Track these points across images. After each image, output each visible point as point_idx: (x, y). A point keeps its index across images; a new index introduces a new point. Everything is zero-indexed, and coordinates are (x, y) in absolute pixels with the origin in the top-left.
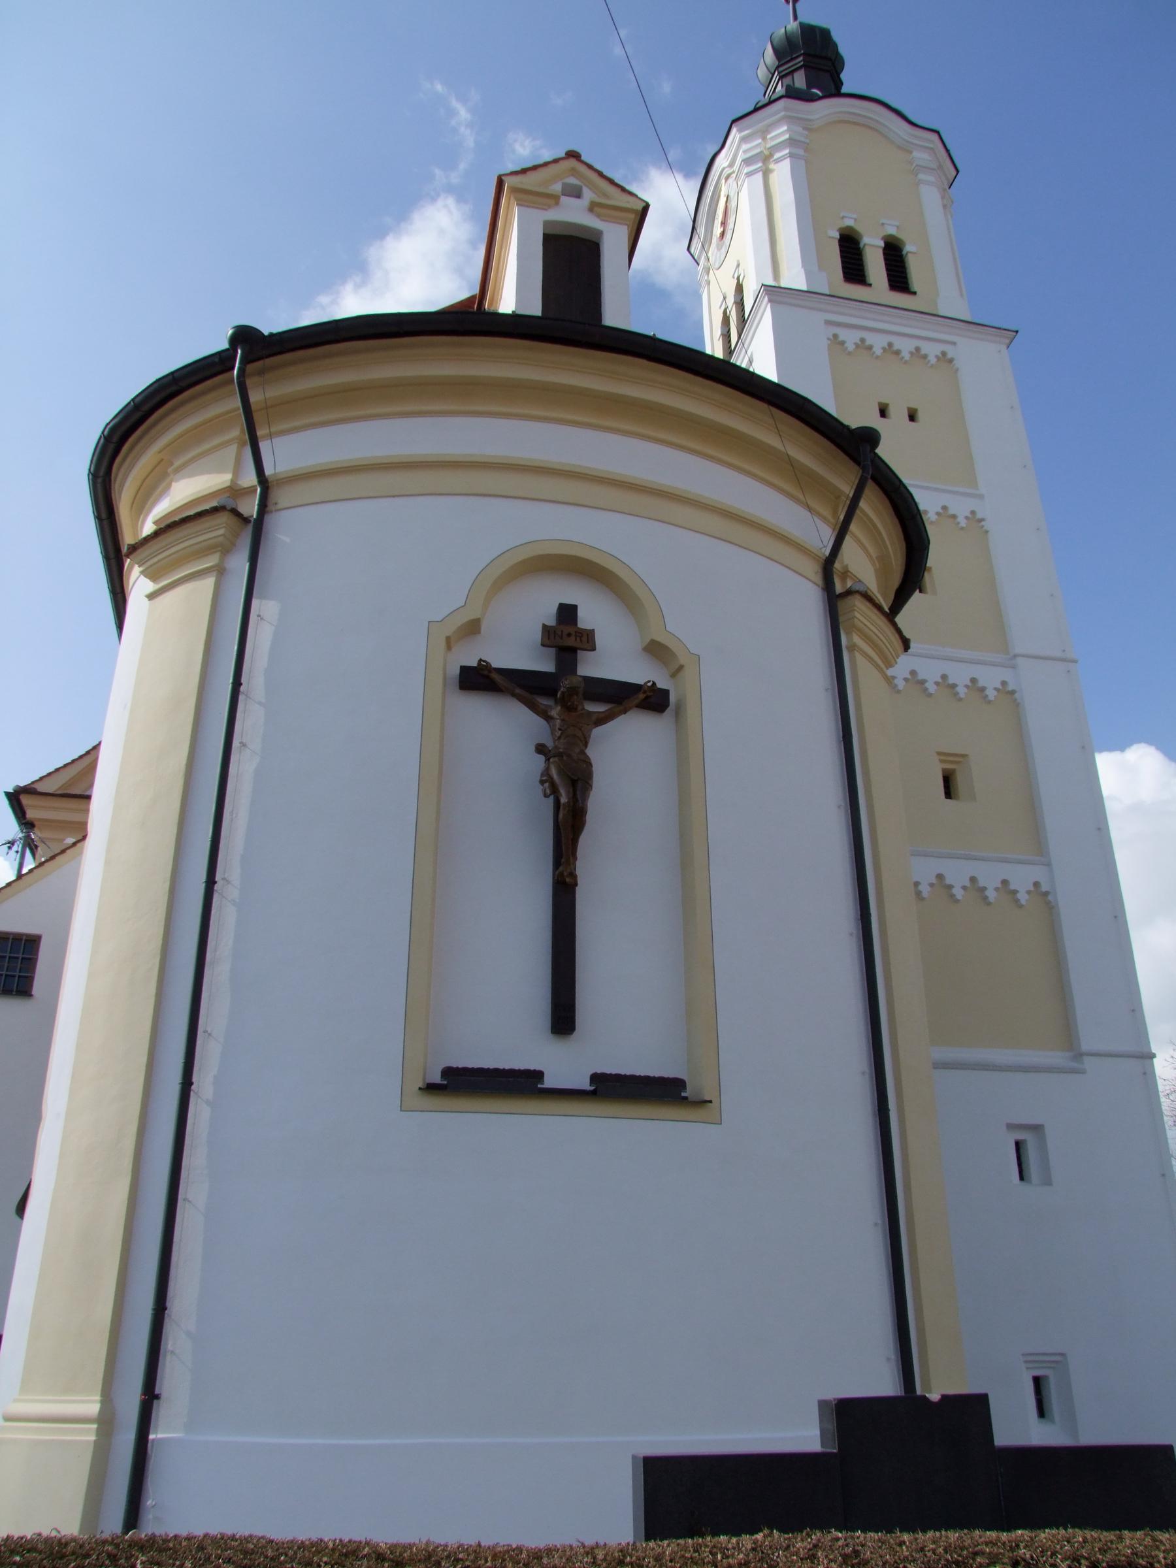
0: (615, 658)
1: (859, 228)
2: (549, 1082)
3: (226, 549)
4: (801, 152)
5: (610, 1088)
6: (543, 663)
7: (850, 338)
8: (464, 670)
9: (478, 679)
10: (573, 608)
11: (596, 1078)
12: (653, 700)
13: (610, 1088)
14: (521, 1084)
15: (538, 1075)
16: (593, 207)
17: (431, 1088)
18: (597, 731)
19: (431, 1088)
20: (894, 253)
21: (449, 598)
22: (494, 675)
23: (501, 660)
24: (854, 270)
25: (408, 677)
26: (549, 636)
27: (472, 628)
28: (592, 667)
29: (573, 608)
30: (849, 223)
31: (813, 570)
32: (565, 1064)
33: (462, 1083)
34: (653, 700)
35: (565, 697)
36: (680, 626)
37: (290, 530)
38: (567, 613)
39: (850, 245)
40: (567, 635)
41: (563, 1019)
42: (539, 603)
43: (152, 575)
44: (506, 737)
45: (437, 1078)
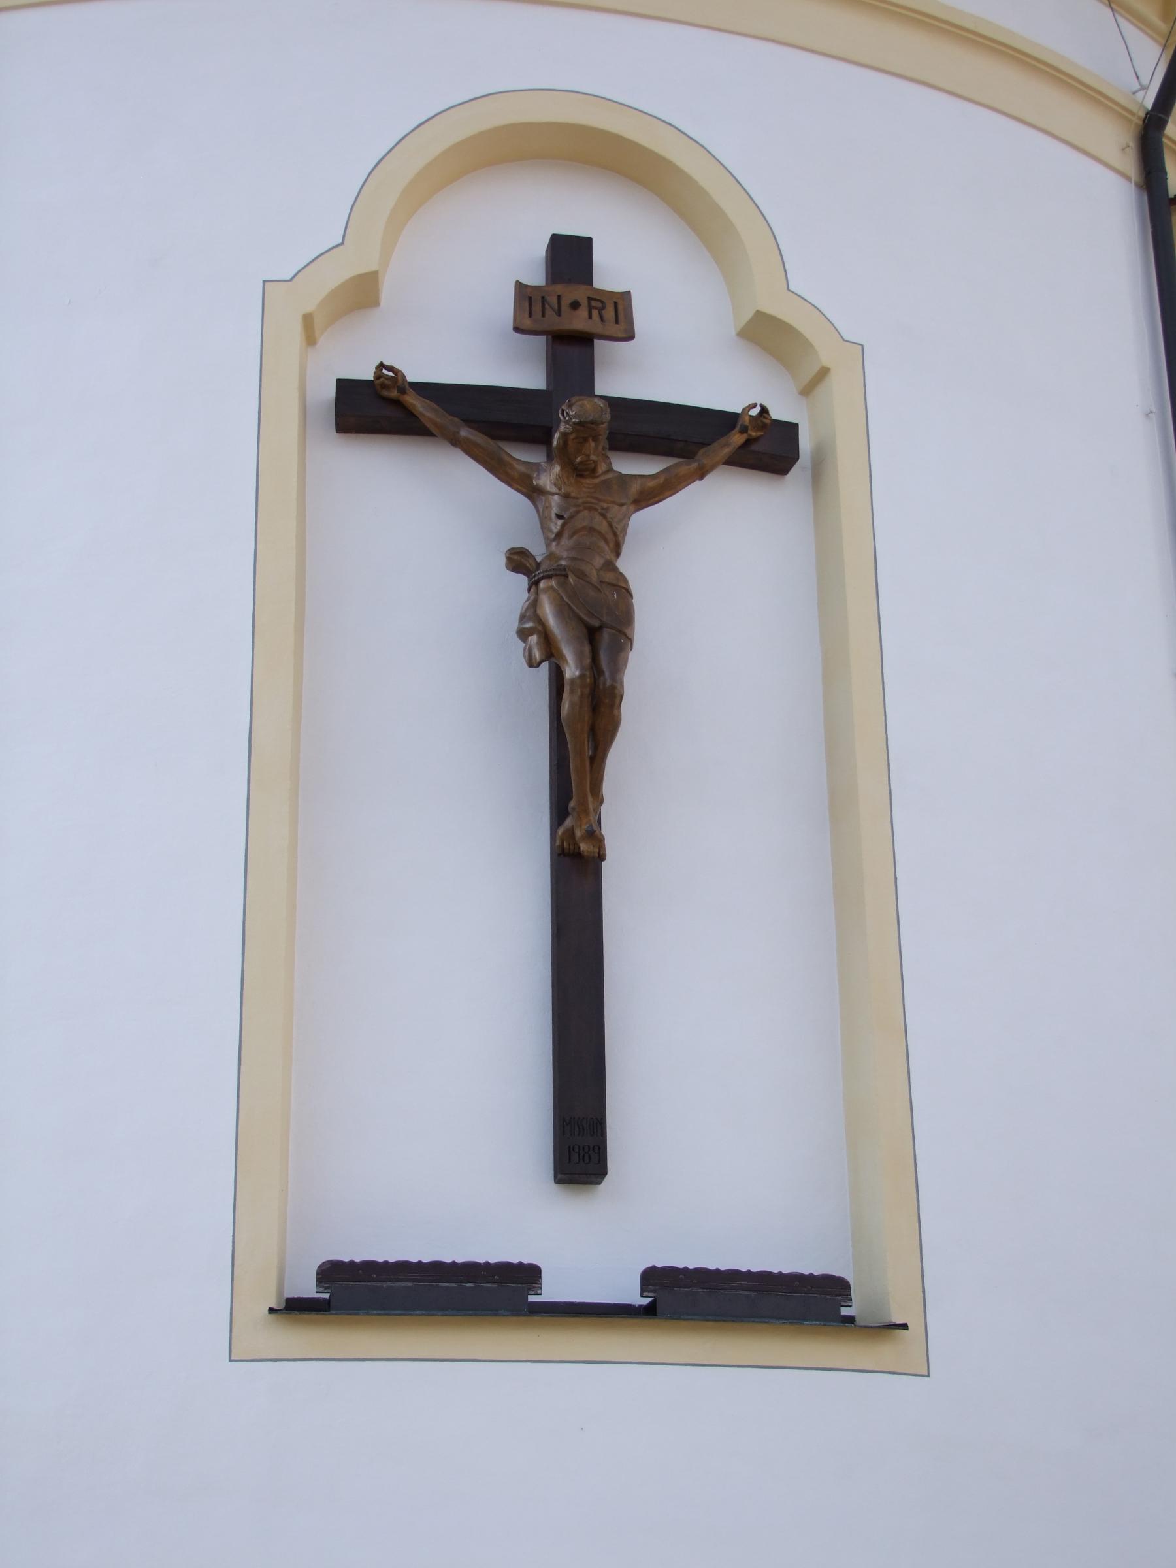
0: (676, 356)
2: (551, 1291)
5: (683, 1298)
6: (520, 370)
8: (346, 388)
9: (376, 408)
10: (584, 244)
11: (652, 1278)
12: (765, 447)
13: (683, 1298)
14: (491, 1294)
15: (530, 1274)
17: (295, 1308)
18: (642, 520)
19: (295, 1308)
21: (305, 219)
22: (413, 401)
23: (427, 364)
27: (361, 295)
28: (625, 375)
29: (584, 244)
31: (1117, 143)
32: (586, 1247)
33: (360, 1293)
34: (765, 447)
36: (820, 281)
38: (570, 256)
40: (569, 304)
41: (580, 1150)
42: (506, 238)
44: (440, 538)
45: (308, 1288)
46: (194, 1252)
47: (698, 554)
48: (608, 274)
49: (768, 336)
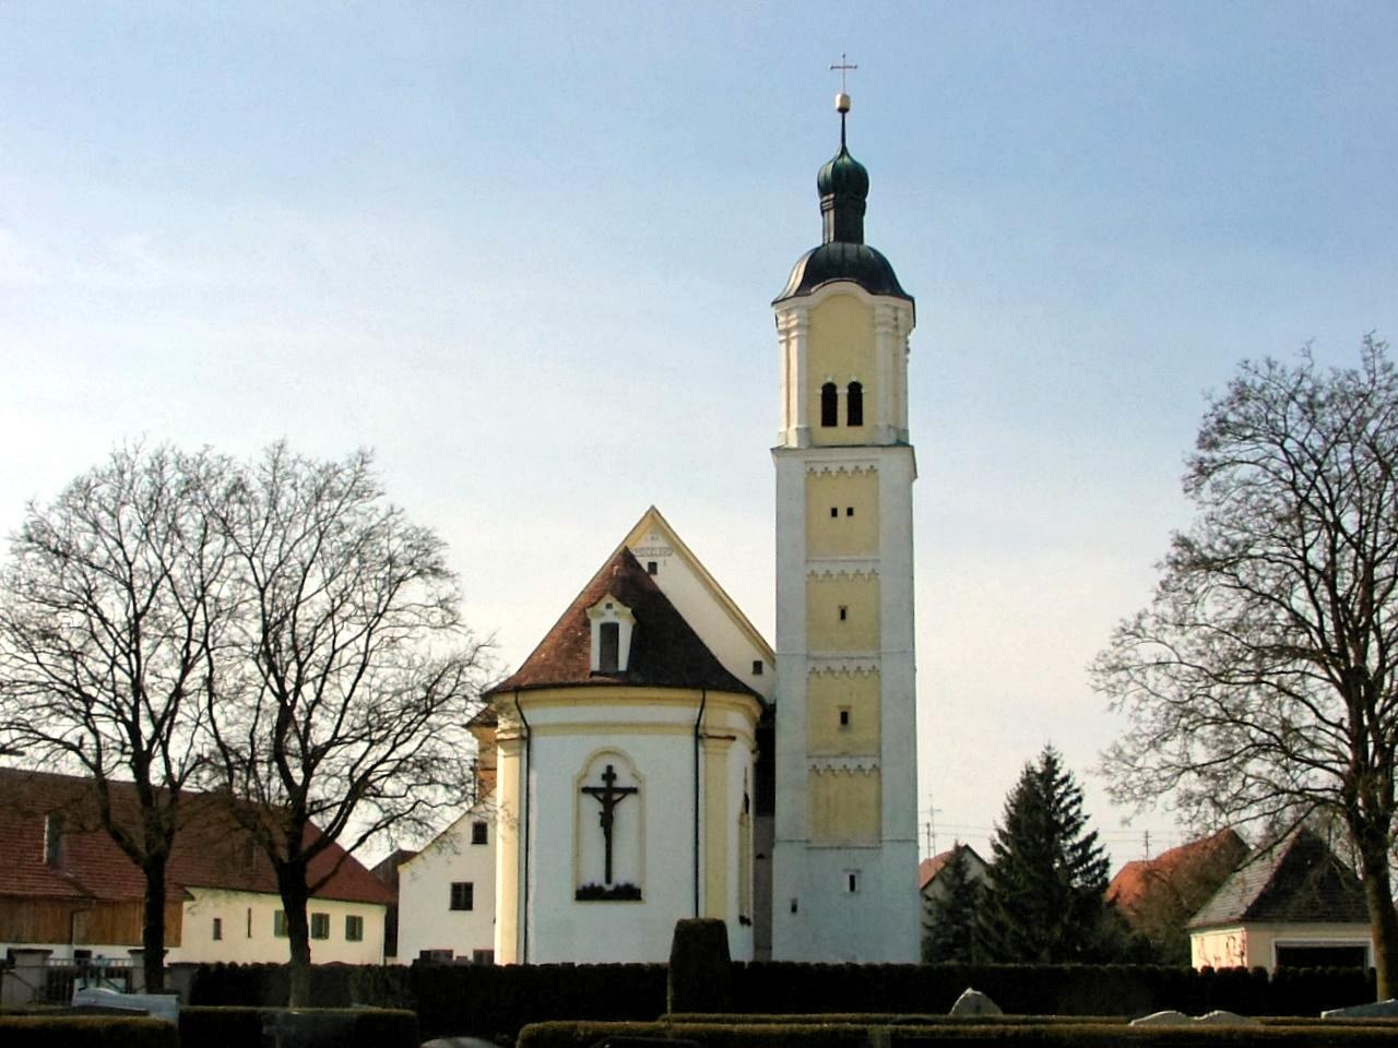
0: (623, 781)
1: (837, 384)
3: (521, 748)
4: (804, 332)
6: (602, 784)
7: (819, 469)
9: (586, 790)
12: (634, 791)
16: (616, 613)
20: (855, 390)
21: (578, 768)
24: (829, 419)
25: (568, 792)
26: (604, 777)
30: (829, 380)
31: (692, 730)
33: (587, 894)
34: (634, 791)
35: (609, 794)
36: (641, 769)
37: (538, 741)
38: (610, 768)
39: (829, 392)
40: (609, 775)
43: (505, 750)
44: (593, 807)
46: (569, 892)
47: (625, 810)
48: (614, 771)
49: (634, 775)
